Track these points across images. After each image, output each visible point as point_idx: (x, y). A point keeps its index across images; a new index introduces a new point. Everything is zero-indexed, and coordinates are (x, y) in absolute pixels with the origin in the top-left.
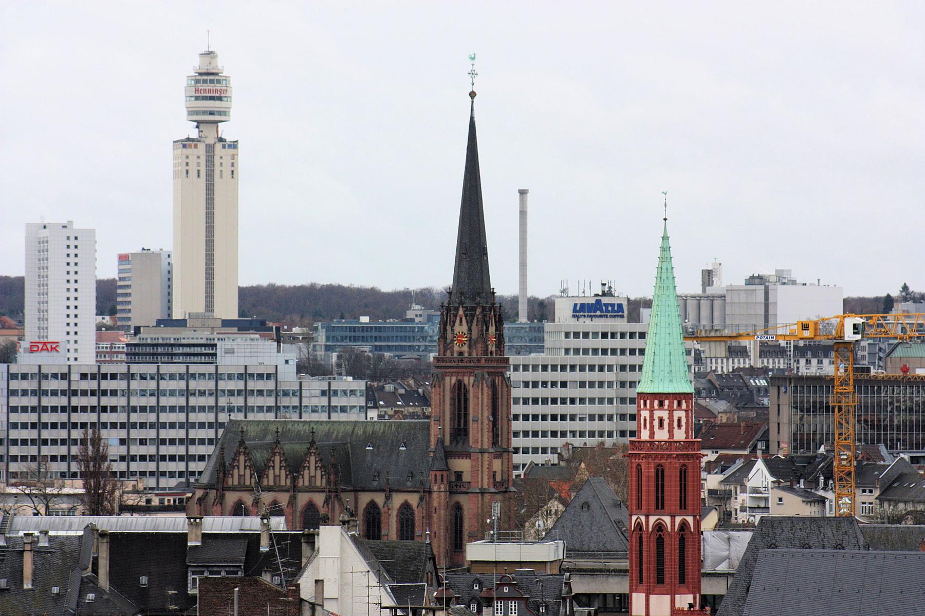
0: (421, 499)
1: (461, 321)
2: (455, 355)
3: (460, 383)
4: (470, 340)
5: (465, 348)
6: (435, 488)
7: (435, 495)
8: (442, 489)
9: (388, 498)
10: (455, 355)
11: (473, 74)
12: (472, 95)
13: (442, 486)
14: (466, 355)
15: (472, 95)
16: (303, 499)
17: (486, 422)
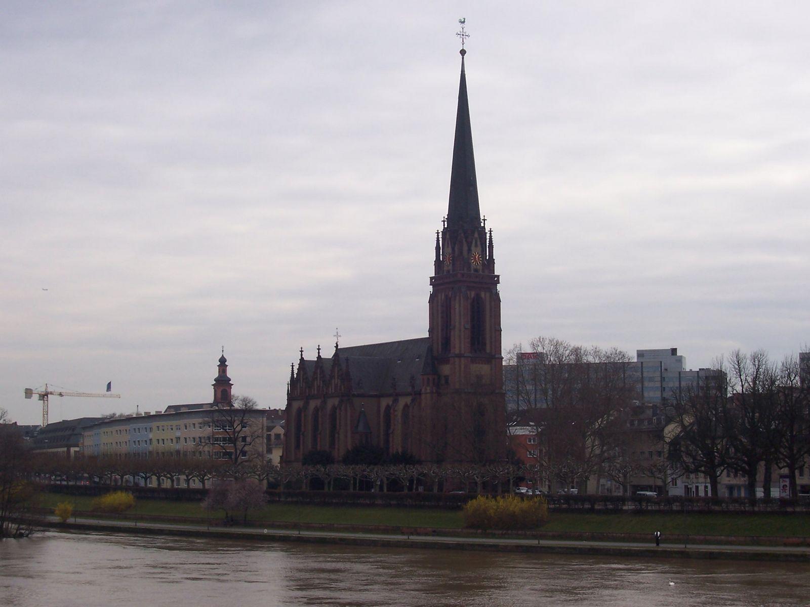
0: (413, 400)
1: (448, 243)
2: (445, 273)
3: (446, 296)
4: (453, 260)
5: (450, 267)
6: (423, 390)
7: (423, 396)
8: (428, 391)
9: (396, 401)
10: (445, 273)
11: (463, 35)
12: (463, 52)
13: (428, 388)
14: (451, 272)
15: (463, 52)
16: (332, 402)
17: (463, 329)
